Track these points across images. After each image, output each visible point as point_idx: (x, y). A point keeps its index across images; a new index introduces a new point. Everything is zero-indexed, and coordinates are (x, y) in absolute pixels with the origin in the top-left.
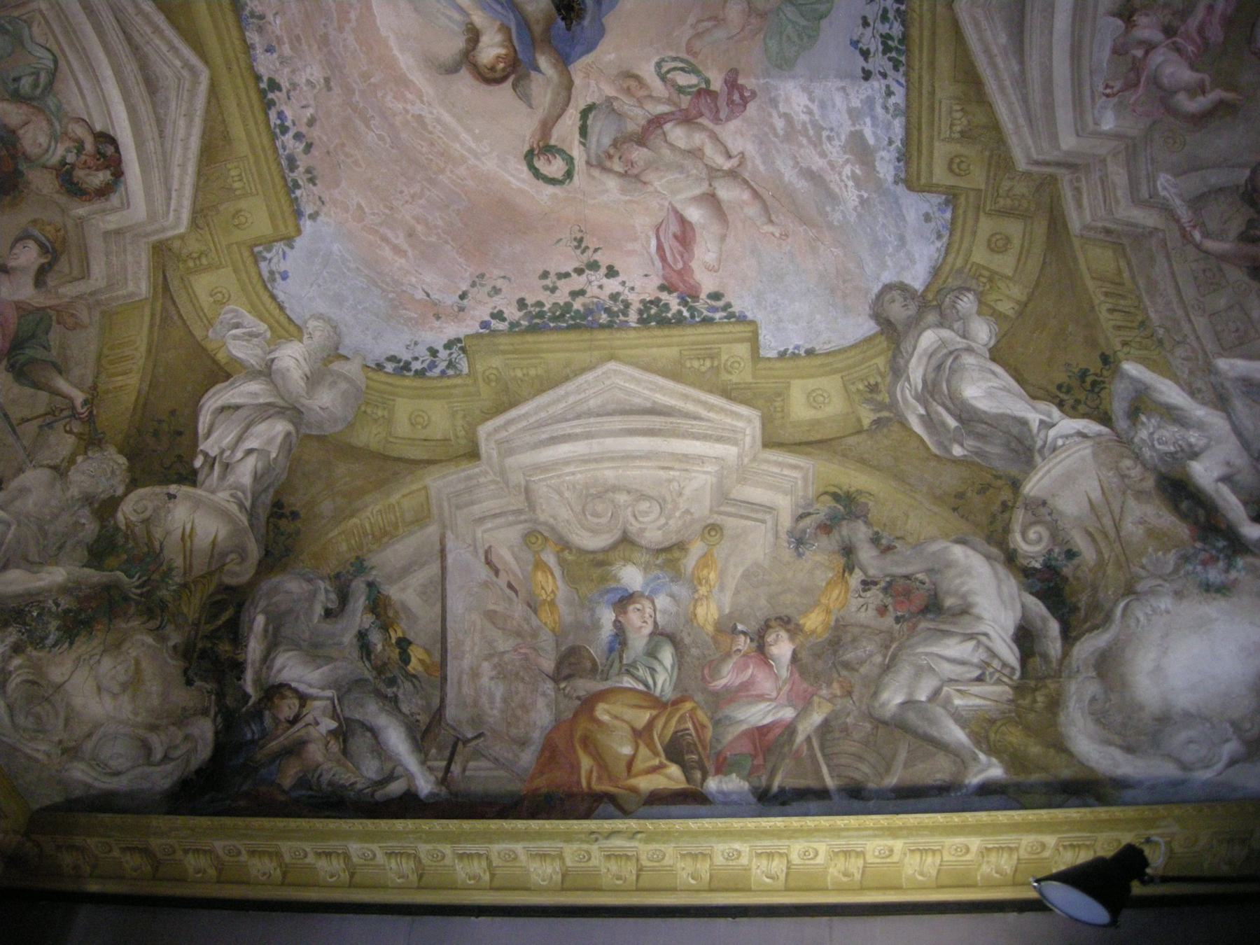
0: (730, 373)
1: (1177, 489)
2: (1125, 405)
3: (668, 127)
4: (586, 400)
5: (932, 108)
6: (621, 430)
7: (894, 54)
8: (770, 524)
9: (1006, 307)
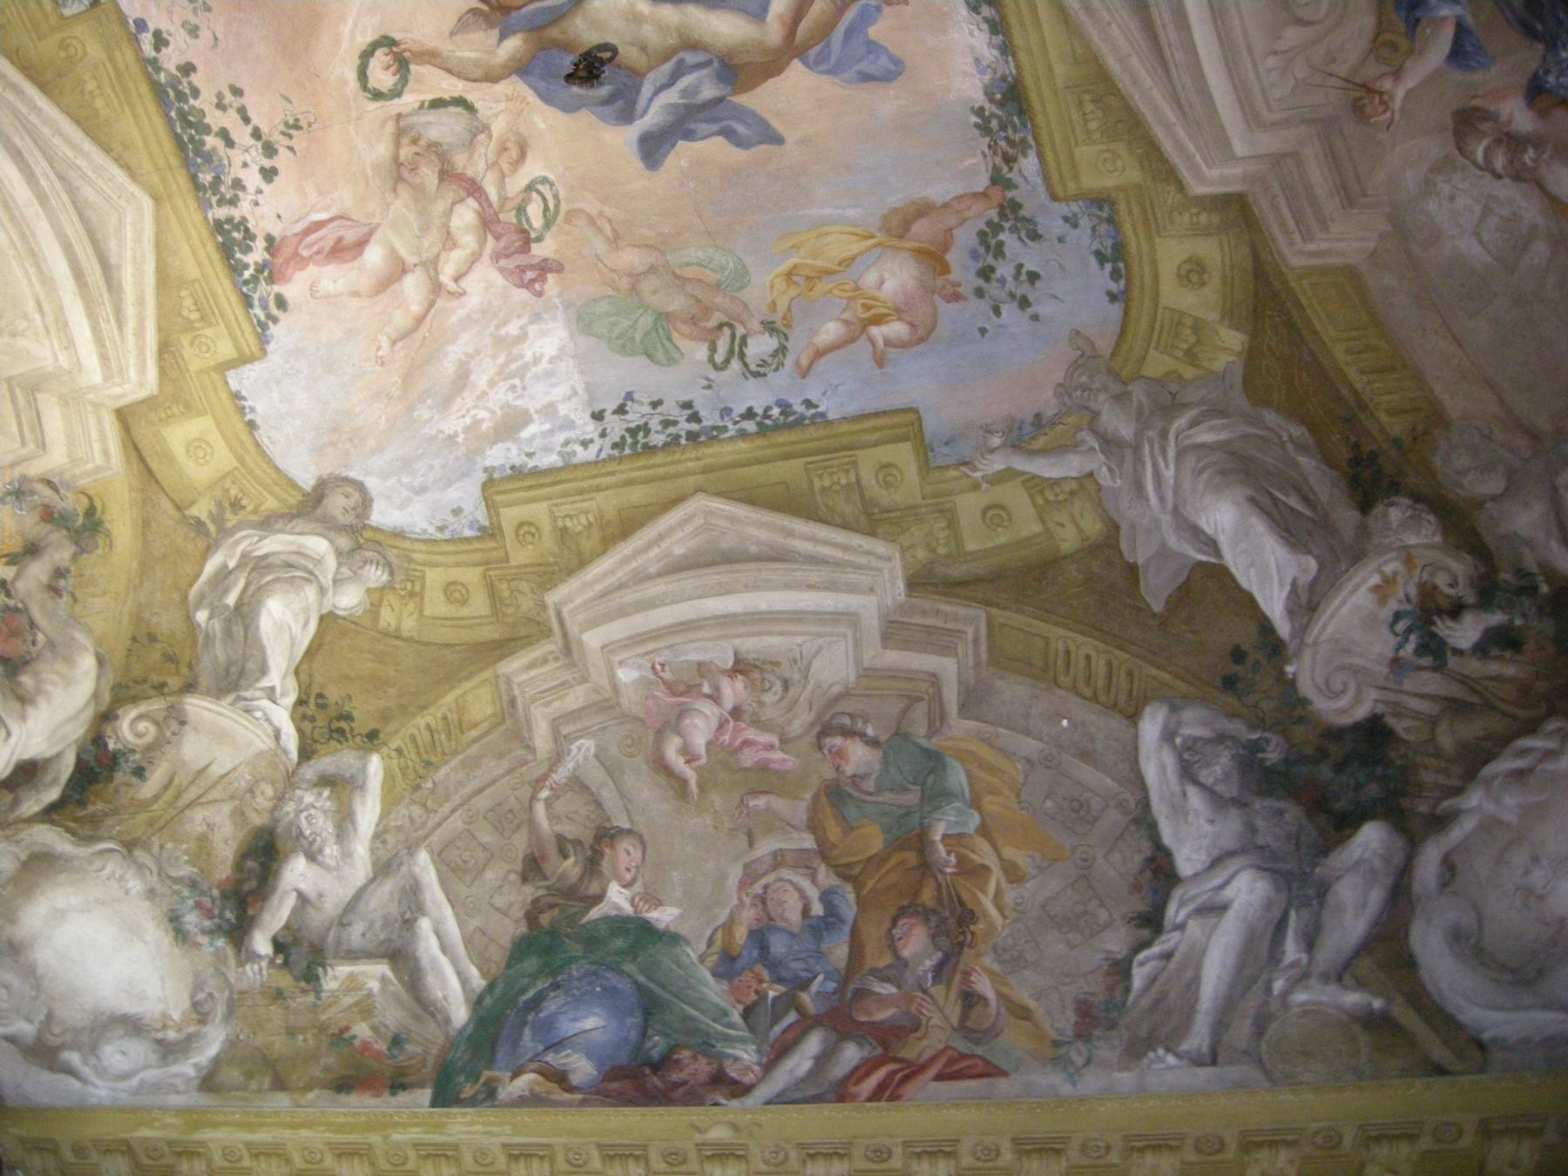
0: (192, 345)
1: (265, 853)
2: (331, 769)
3: (472, 202)
4: (83, 176)
5: (581, 492)
6: (66, 236)
7: (629, 440)
8: (24, 451)
9: (387, 618)
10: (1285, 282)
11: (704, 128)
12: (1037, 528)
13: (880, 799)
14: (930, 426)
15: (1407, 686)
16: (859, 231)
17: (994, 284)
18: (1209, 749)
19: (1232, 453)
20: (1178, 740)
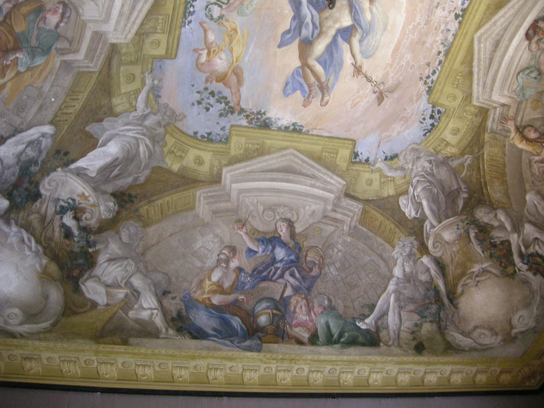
10: (192, 188)
11: (294, 24)
12: (123, 91)
13: (35, 29)
14: (168, 62)
15: (50, 204)
16: (240, 58)
17: (208, 95)
18: (37, 149)
19: (135, 156)
20: (41, 139)
